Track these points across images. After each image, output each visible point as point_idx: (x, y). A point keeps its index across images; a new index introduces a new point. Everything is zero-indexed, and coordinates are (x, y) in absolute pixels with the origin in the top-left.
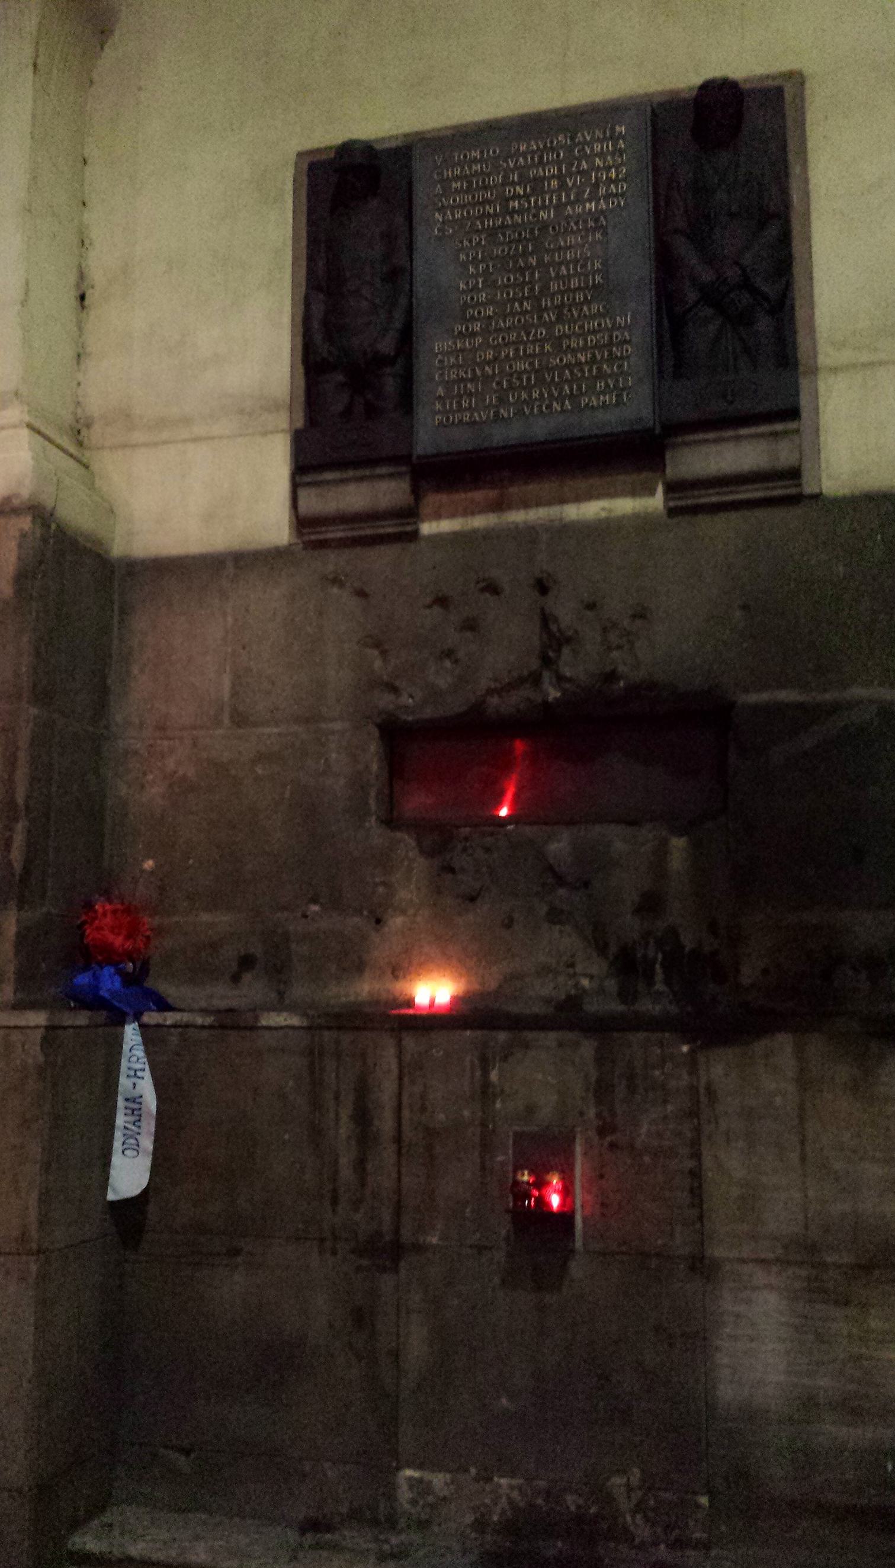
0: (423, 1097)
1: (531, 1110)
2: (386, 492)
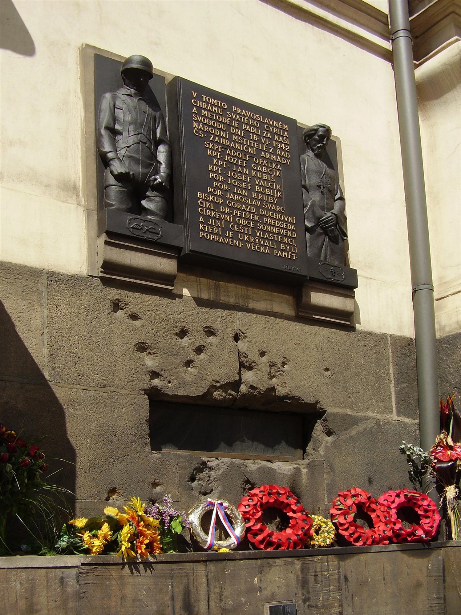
2: (166, 265)
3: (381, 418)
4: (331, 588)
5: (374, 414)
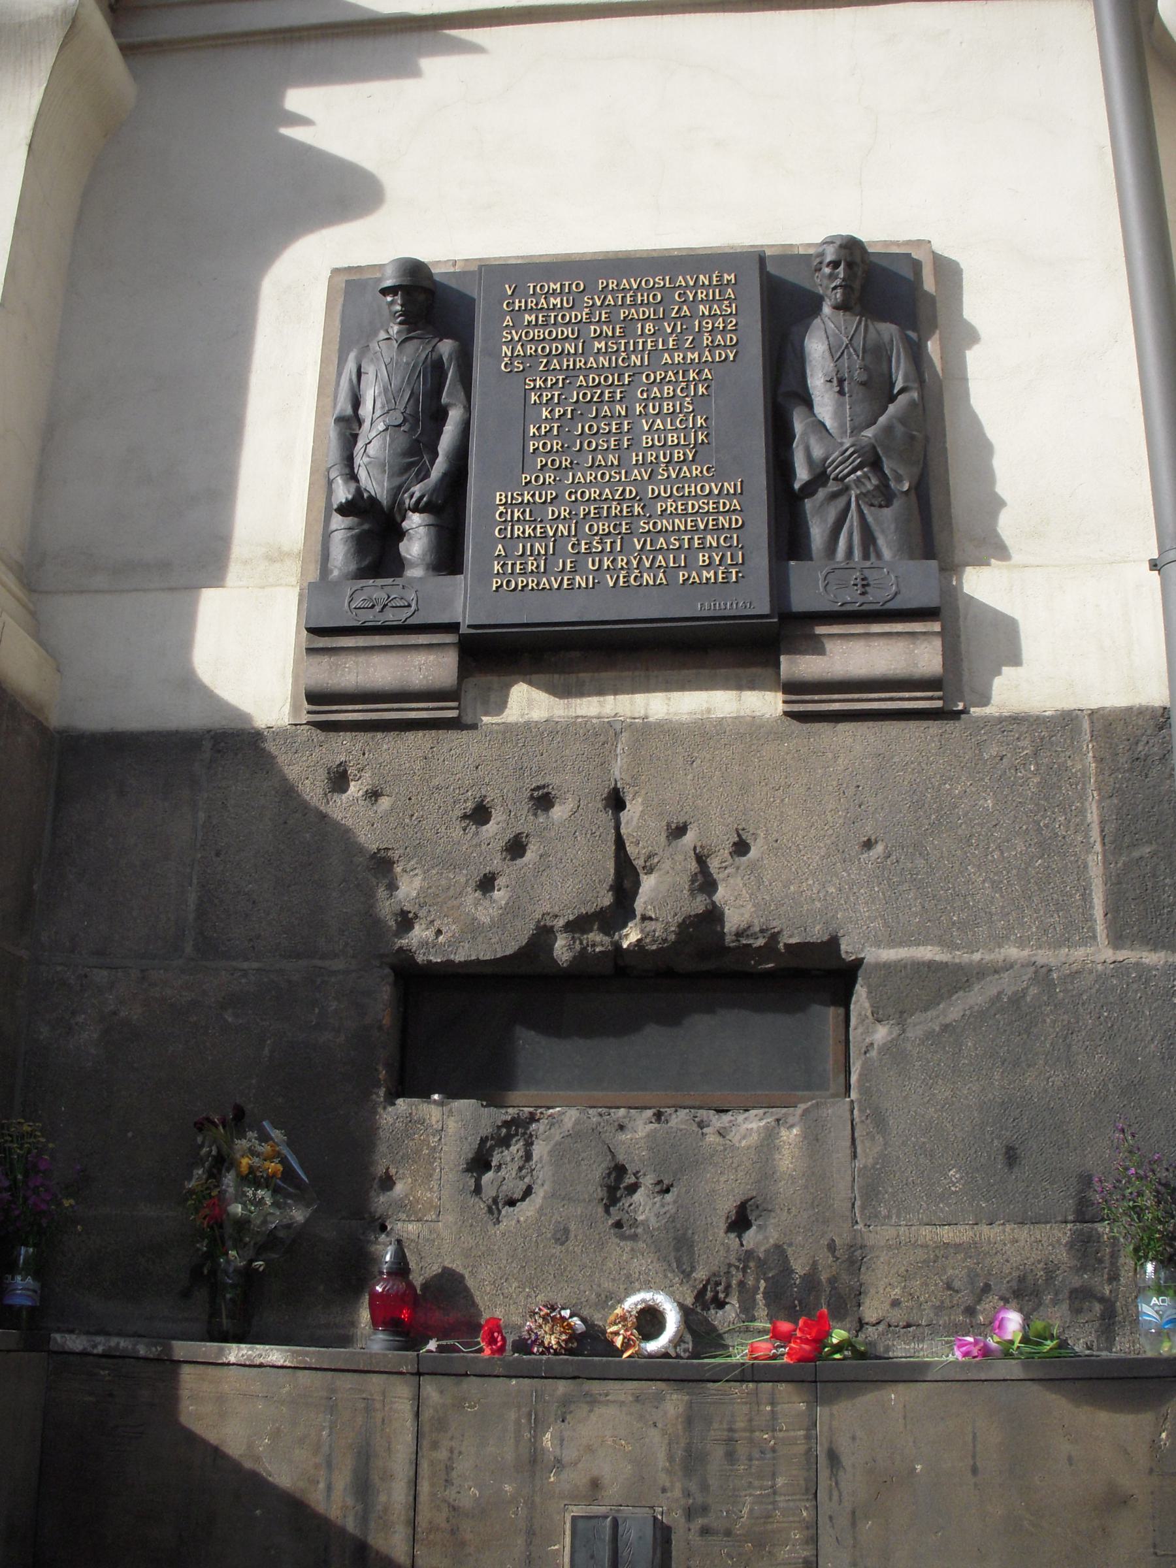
0: (449, 1469)
1: (595, 1484)
3: (1053, 962)
4: (780, 1481)
5: (1026, 953)
